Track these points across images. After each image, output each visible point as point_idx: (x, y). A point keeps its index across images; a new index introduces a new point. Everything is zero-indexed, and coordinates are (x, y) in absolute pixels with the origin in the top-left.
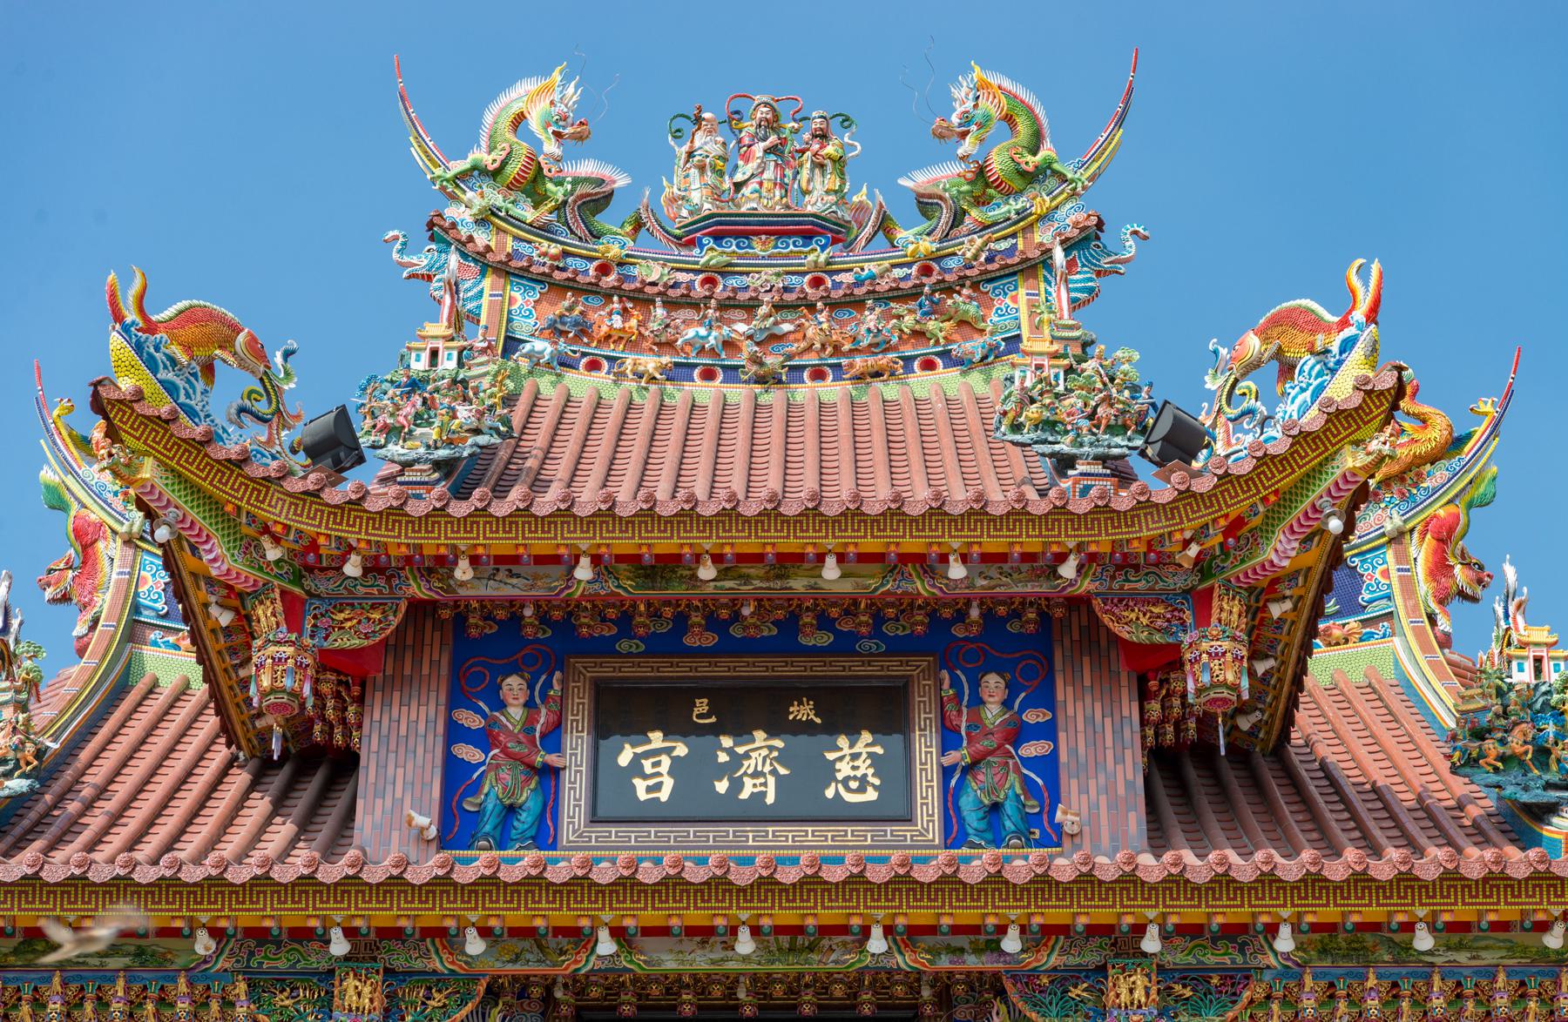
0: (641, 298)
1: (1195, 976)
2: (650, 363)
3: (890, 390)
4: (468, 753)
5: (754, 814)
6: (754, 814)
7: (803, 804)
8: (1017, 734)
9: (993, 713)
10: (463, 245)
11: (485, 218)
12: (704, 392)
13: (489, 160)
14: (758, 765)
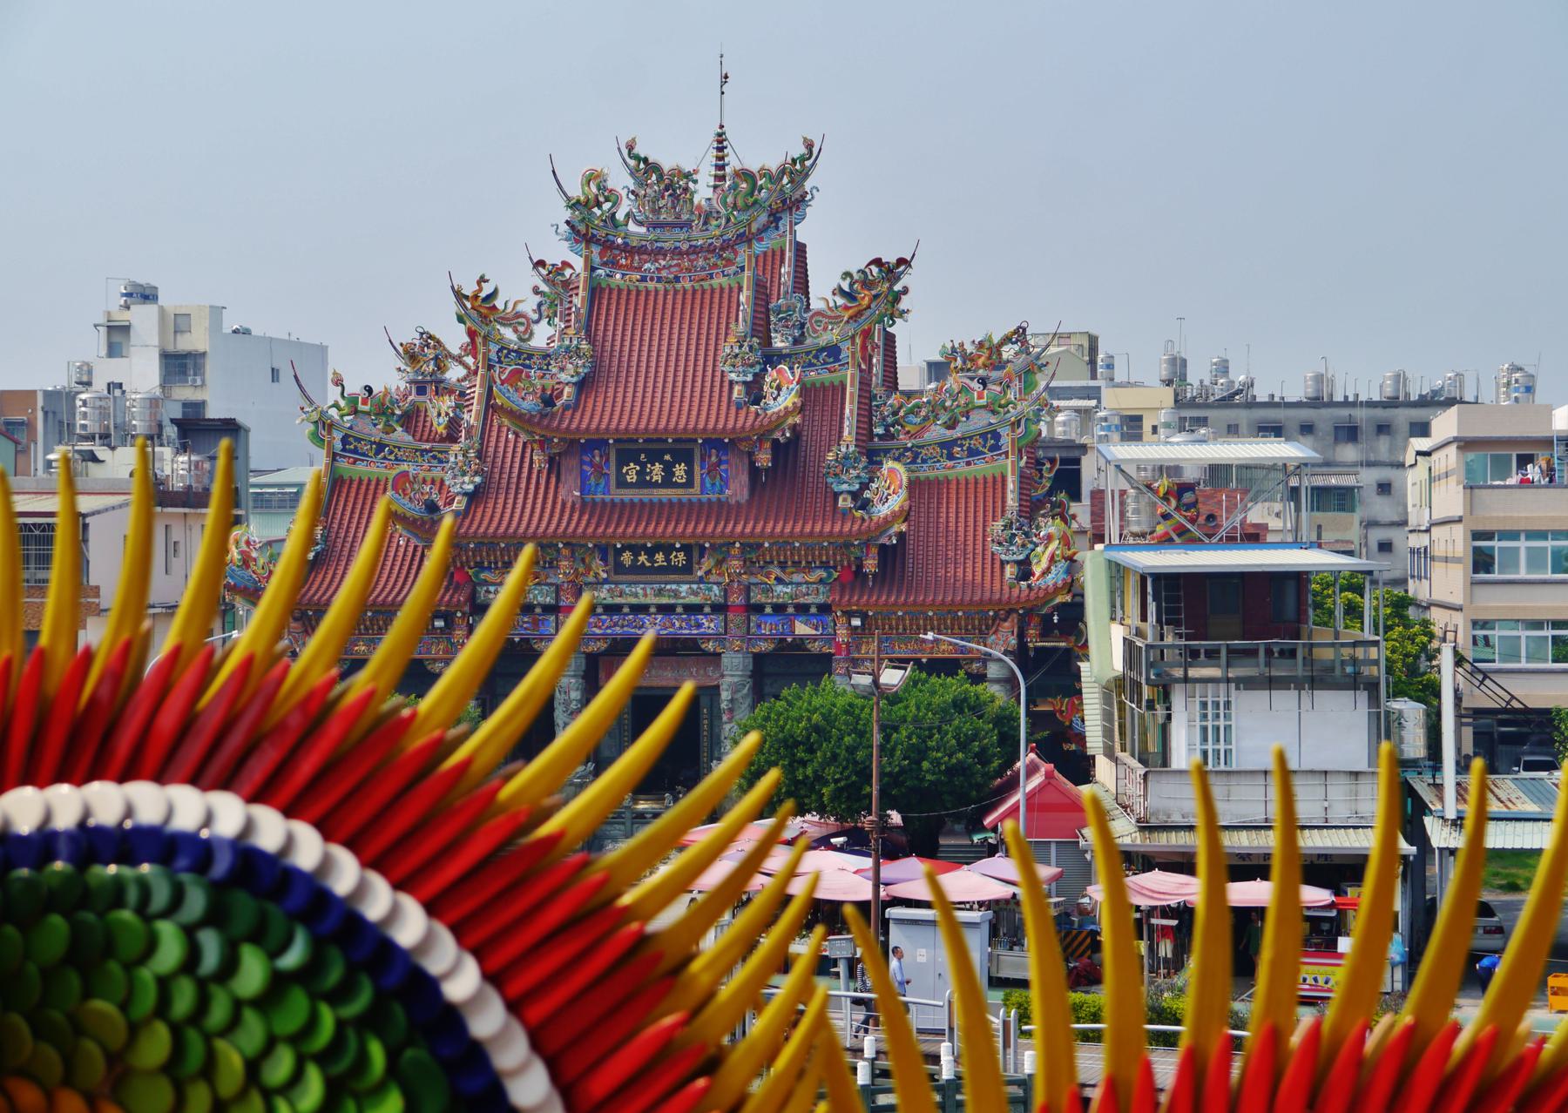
1: (750, 546)
3: (706, 284)
4: (586, 468)
5: (656, 485)
6: (656, 485)
7: (668, 482)
9: (714, 459)
12: (651, 285)
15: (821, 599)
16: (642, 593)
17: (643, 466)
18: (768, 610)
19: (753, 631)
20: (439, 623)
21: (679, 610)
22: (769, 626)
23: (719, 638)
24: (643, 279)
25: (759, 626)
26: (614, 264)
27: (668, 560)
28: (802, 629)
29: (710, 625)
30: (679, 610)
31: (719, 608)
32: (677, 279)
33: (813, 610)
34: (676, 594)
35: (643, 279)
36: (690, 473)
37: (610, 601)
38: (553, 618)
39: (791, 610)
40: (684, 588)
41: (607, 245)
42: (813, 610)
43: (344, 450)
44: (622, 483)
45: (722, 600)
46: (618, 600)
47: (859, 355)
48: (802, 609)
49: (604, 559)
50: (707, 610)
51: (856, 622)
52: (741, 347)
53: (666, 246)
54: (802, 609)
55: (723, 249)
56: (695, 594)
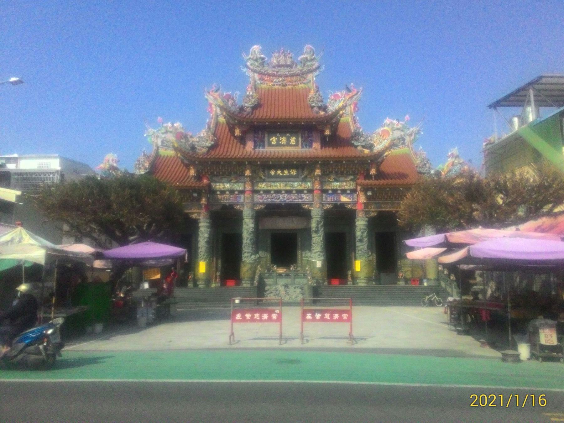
0: (269, 75)
2: (271, 84)
3: (297, 87)
4: (256, 139)
5: (283, 145)
6: (283, 145)
7: (288, 144)
8: (309, 137)
10: (249, 68)
11: (251, 65)
13: (252, 57)
14: (284, 140)
15: (352, 187)
16: (279, 186)
17: (278, 138)
18: (330, 192)
19: (324, 200)
20: (195, 195)
21: (294, 192)
22: (330, 199)
23: (311, 204)
24: (274, 85)
25: (327, 198)
26: (263, 80)
27: (289, 173)
28: (344, 199)
29: (306, 197)
30: (294, 192)
31: (310, 191)
32: (286, 85)
33: (348, 192)
34: (292, 186)
35: (274, 85)
36: (297, 141)
37: (266, 188)
38: (242, 196)
39: (339, 192)
40: (296, 183)
41: (260, 73)
42: (348, 192)
43: (162, 145)
44: (270, 144)
45: (311, 188)
46: (269, 188)
47: (352, 111)
48: (344, 192)
49: (264, 171)
50: (305, 192)
51: (369, 193)
52: (315, 95)
53: (282, 73)
54: (344, 192)
55: (303, 74)
56: (301, 185)
